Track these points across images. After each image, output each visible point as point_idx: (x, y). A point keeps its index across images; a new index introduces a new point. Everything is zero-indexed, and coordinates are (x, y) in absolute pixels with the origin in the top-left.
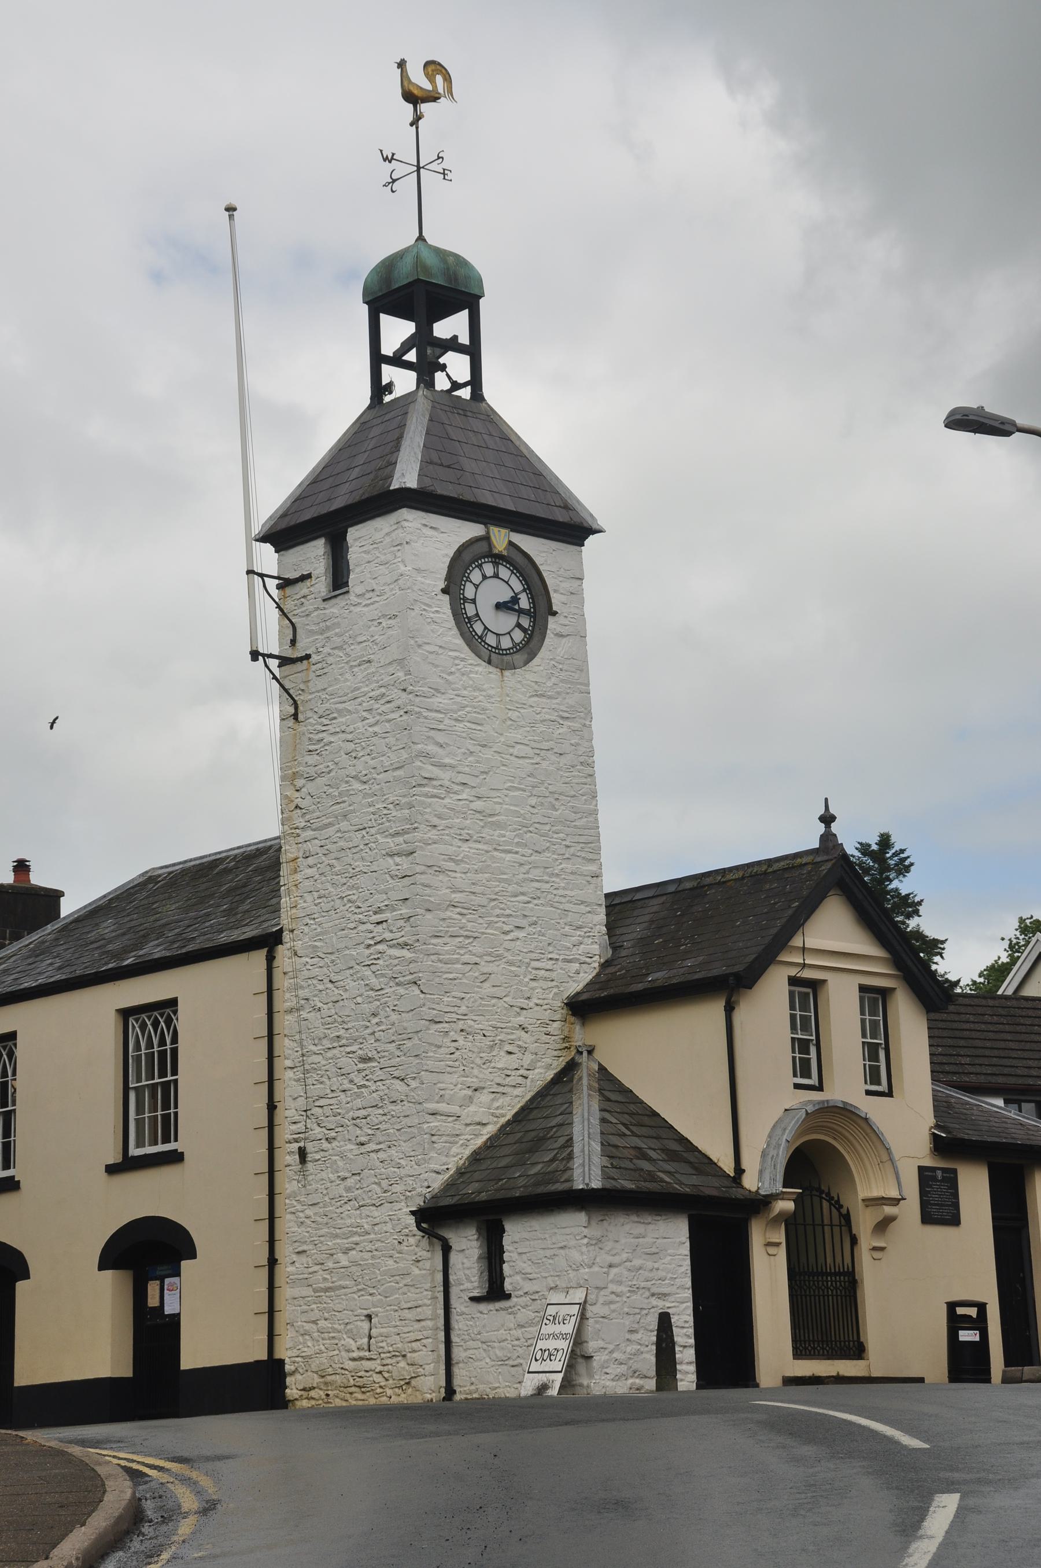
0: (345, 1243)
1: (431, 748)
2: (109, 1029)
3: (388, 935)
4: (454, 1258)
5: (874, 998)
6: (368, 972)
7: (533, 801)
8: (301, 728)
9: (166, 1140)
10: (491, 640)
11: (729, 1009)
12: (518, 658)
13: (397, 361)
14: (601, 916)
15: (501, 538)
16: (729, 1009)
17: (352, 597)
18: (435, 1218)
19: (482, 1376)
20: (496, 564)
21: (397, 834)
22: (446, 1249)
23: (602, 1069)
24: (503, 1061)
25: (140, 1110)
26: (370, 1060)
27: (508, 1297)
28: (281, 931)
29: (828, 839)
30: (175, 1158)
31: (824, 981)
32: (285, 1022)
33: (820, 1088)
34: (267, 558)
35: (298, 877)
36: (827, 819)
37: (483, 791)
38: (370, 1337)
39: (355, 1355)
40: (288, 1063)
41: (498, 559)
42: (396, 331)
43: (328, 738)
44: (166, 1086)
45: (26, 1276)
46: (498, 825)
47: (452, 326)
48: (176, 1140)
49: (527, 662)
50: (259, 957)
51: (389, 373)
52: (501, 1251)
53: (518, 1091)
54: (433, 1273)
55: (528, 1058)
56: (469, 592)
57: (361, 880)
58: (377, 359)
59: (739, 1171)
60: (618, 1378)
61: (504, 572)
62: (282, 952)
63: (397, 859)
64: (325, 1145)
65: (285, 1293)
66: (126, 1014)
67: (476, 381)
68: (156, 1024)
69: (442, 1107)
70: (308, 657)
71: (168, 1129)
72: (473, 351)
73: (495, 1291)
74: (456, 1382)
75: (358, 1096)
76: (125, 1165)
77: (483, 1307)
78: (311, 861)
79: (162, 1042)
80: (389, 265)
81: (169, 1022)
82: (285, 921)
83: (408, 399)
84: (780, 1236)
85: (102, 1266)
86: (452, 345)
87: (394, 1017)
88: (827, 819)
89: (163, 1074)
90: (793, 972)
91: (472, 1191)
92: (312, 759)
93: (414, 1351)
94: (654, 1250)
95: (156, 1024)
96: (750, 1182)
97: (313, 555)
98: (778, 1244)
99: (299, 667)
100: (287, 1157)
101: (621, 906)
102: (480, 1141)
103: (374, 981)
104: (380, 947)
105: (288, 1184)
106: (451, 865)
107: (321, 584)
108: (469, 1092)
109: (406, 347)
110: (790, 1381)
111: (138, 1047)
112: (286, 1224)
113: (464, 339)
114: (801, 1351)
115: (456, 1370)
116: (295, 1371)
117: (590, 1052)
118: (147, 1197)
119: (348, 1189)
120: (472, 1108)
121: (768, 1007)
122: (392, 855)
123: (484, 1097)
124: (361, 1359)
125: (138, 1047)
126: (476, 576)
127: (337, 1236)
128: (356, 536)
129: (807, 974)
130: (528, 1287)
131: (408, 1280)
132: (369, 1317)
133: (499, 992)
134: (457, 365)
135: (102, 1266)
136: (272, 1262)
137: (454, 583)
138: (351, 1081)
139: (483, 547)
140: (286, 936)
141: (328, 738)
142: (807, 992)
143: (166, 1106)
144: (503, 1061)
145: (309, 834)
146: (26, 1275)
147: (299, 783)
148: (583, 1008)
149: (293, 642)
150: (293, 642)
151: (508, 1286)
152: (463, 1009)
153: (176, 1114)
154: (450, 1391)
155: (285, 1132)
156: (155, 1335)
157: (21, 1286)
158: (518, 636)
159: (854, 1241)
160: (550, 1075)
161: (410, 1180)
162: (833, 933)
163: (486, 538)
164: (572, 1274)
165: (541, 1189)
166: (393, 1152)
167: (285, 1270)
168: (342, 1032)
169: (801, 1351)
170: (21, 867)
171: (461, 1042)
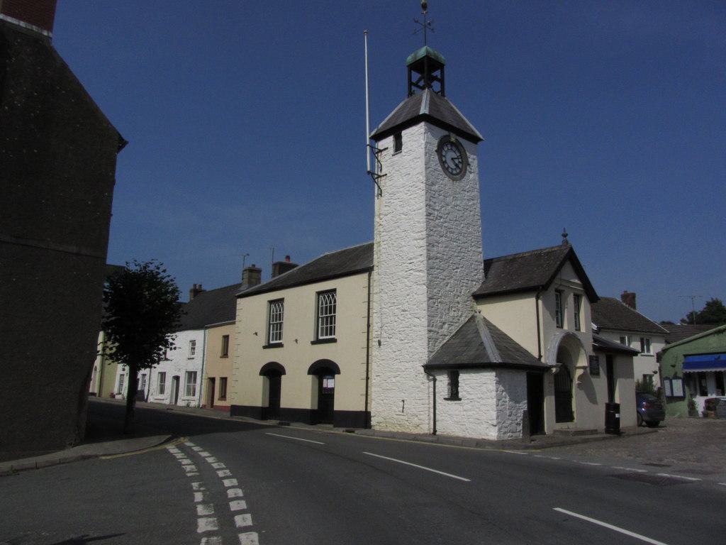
0: (395, 374)
2: (313, 297)
3: (414, 267)
9: (331, 334)
13: (416, 85)
17: (403, 153)
20: (451, 146)
21: (419, 232)
22: (435, 380)
25: (322, 324)
26: (404, 311)
27: (460, 400)
28: (373, 266)
30: (334, 341)
32: (375, 298)
35: (381, 248)
36: (565, 236)
37: (448, 220)
38: (403, 408)
39: (398, 413)
40: (374, 311)
41: (452, 144)
42: (416, 76)
43: (392, 201)
45: (284, 373)
46: (453, 233)
47: (437, 73)
49: (460, 179)
50: (365, 275)
51: (414, 88)
52: (458, 382)
53: (457, 324)
54: (429, 387)
55: (460, 313)
56: (444, 153)
57: (405, 248)
58: (411, 84)
59: (540, 356)
61: (454, 149)
62: (374, 273)
64: (388, 340)
65: (372, 390)
66: (319, 293)
68: (329, 297)
70: (386, 175)
72: (442, 81)
73: (454, 396)
76: (317, 342)
77: (449, 402)
78: (385, 243)
79: (331, 303)
81: (333, 296)
82: (375, 263)
84: (552, 379)
86: (435, 78)
87: (416, 296)
88: (565, 236)
89: (330, 313)
90: (556, 287)
91: (446, 360)
92: (386, 209)
95: (329, 297)
97: (389, 142)
99: (383, 178)
100: (374, 343)
103: (408, 284)
104: (412, 272)
105: (374, 352)
107: (391, 151)
109: (420, 80)
111: (322, 304)
112: (373, 366)
114: (558, 421)
115: (437, 423)
117: (480, 312)
118: (324, 352)
119: (397, 356)
122: (416, 240)
124: (400, 415)
125: (322, 304)
126: (446, 149)
128: (404, 133)
129: (561, 288)
130: (469, 396)
132: (403, 401)
133: (452, 290)
136: (367, 378)
138: (398, 318)
140: (375, 268)
141: (392, 201)
143: (331, 323)
144: (452, 314)
145: (385, 233)
146: (284, 373)
147: (381, 217)
151: (460, 395)
152: (440, 295)
154: (435, 431)
155: (374, 334)
156: (326, 397)
157: (283, 377)
160: (467, 319)
161: (421, 354)
164: (489, 394)
165: (477, 361)
166: (414, 344)
167: (373, 381)
168: (395, 301)
169: (558, 421)
170: (288, 257)
171: (439, 305)
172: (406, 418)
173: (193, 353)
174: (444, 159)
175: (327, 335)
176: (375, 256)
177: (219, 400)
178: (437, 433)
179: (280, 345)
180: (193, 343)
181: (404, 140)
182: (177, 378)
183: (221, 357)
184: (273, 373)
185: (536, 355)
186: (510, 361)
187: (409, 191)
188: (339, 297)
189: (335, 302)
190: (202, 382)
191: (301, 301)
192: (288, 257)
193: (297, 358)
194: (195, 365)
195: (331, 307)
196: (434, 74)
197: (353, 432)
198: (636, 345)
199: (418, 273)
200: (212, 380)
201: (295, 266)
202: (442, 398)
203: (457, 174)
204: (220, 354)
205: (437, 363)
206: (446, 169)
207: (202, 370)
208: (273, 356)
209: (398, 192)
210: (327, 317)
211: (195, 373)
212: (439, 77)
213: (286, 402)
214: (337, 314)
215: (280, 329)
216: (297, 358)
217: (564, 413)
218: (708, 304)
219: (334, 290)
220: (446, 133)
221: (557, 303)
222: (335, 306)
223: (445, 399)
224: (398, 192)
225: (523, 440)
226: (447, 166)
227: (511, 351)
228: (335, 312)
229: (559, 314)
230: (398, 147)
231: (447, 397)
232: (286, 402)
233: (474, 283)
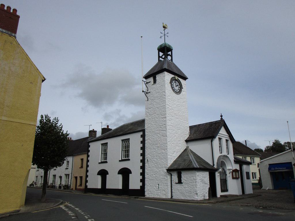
1: (168, 104)
3: (162, 129)
4: (172, 177)
5: (227, 141)
6: (158, 135)
7: (181, 112)
8: (148, 102)
10: (175, 90)
11: (212, 141)
12: (179, 93)
13: (161, 57)
14: (189, 129)
15: (177, 78)
16: (212, 141)
17: (157, 84)
18: (170, 171)
19: (177, 196)
22: (171, 175)
23: (190, 150)
24: (177, 148)
26: (159, 147)
27: (182, 183)
29: (222, 119)
30: (129, 160)
31: (222, 138)
33: (222, 153)
34: (144, 80)
36: (221, 116)
37: (175, 110)
39: (156, 190)
41: (176, 80)
42: (161, 54)
44: (127, 150)
47: (170, 53)
48: (129, 157)
51: (160, 59)
52: (181, 176)
57: (157, 122)
58: (159, 57)
59: (214, 165)
60: (201, 197)
61: (177, 82)
63: (163, 119)
64: (151, 159)
66: (122, 140)
67: (172, 60)
68: (126, 142)
69: (170, 154)
71: (128, 156)
72: (171, 56)
73: (180, 182)
74: (173, 195)
75: (157, 152)
76: (122, 160)
77: (178, 184)
79: (127, 144)
80: (161, 46)
83: (163, 61)
84: (219, 175)
85: (118, 174)
86: (169, 55)
87: (163, 141)
88: (221, 116)
91: (175, 167)
93: (166, 190)
94: (205, 177)
95: (126, 142)
96: (215, 167)
97: (151, 79)
98: (218, 176)
101: (191, 128)
102: (175, 159)
103: (159, 136)
104: (161, 131)
106: (171, 120)
107: (153, 83)
108: (173, 152)
109: (163, 56)
110: (221, 196)
111: (124, 145)
113: (170, 54)
115: (173, 194)
116: (147, 191)
120: (174, 155)
121: (216, 141)
123: (175, 153)
125: (124, 145)
126: (173, 82)
127: (153, 172)
130: (186, 182)
131: (165, 179)
134: (169, 58)
135: (118, 174)
137: (171, 82)
139: (174, 78)
142: (220, 139)
144: (177, 148)
148: (187, 141)
149: (148, 91)
150: (148, 91)
151: (182, 181)
152: (173, 140)
153: (129, 154)
157: (107, 175)
158: (179, 91)
159: (226, 175)
162: (223, 131)
163: (175, 77)
165: (188, 167)
170: (108, 126)
172: (160, 191)
173: (68, 166)
174: (173, 86)
175: (126, 157)
176: (146, 125)
177: (79, 186)
178: (173, 198)
179: (106, 162)
180: (82, 160)
181: (157, 78)
182: (61, 177)
183: (80, 168)
184: (103, 174)
185: (212, 164)
186: (202, 167)
187: (159, 99)
188: (131, 142)
189: (129, 144)
190: (71, 178)
191: (115, 145)
192: (108, 126)
193: (114, 166)
194: (69, 171)
195: (127, 146)
196: (169, 53)
197: (138, 198)
198: (248, 159)
199: (163, 132)
200: (76, 178)
201: (111, 129)
202: (175, 183)
203: (178, 92)
204: (80, 167)
205: (172, 168)
206: (174, 90)
207: (72, 173)
208: (103, 167)
209: (155, 99)
210: (126, 150)
211: (69, 175)
212: (170, 54)
213: (108, 186)
214: (130, 149)
215: (106, 155)
216: (114, 166)
217: (224, 188)
218: (274, 143)
219: (129, 139)
220: (173, 76)
221: (219, 143)
222: (129, 146)
223: (176, 183)
224: (155, 99)
225: (209, 199)
226: (174, 89)
227: (202, 163)
228: (129, 148)
229: (220, 148)
230: (155, 82)
231: (177, 182)
232: (108, 186)
233: (186, 135)
